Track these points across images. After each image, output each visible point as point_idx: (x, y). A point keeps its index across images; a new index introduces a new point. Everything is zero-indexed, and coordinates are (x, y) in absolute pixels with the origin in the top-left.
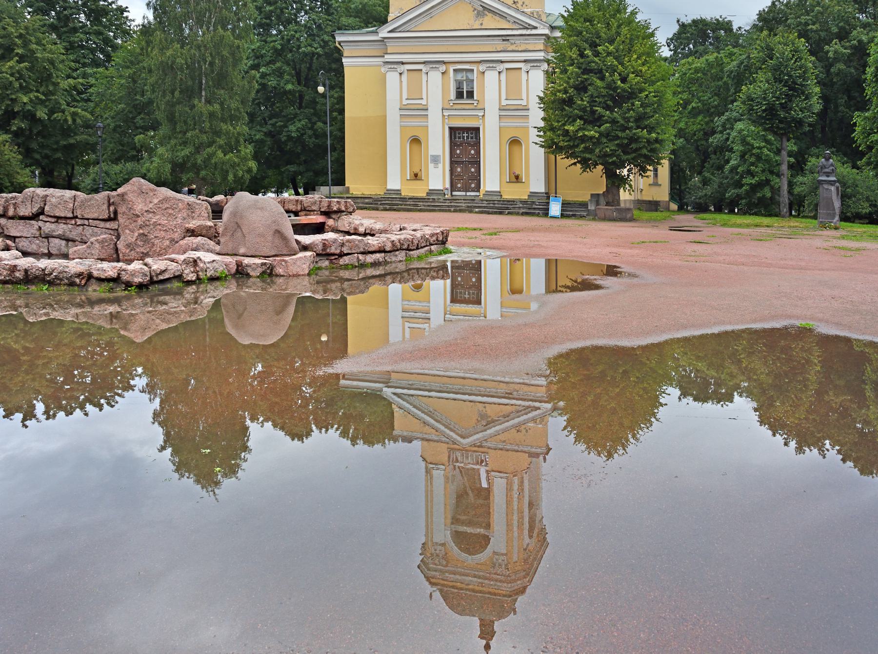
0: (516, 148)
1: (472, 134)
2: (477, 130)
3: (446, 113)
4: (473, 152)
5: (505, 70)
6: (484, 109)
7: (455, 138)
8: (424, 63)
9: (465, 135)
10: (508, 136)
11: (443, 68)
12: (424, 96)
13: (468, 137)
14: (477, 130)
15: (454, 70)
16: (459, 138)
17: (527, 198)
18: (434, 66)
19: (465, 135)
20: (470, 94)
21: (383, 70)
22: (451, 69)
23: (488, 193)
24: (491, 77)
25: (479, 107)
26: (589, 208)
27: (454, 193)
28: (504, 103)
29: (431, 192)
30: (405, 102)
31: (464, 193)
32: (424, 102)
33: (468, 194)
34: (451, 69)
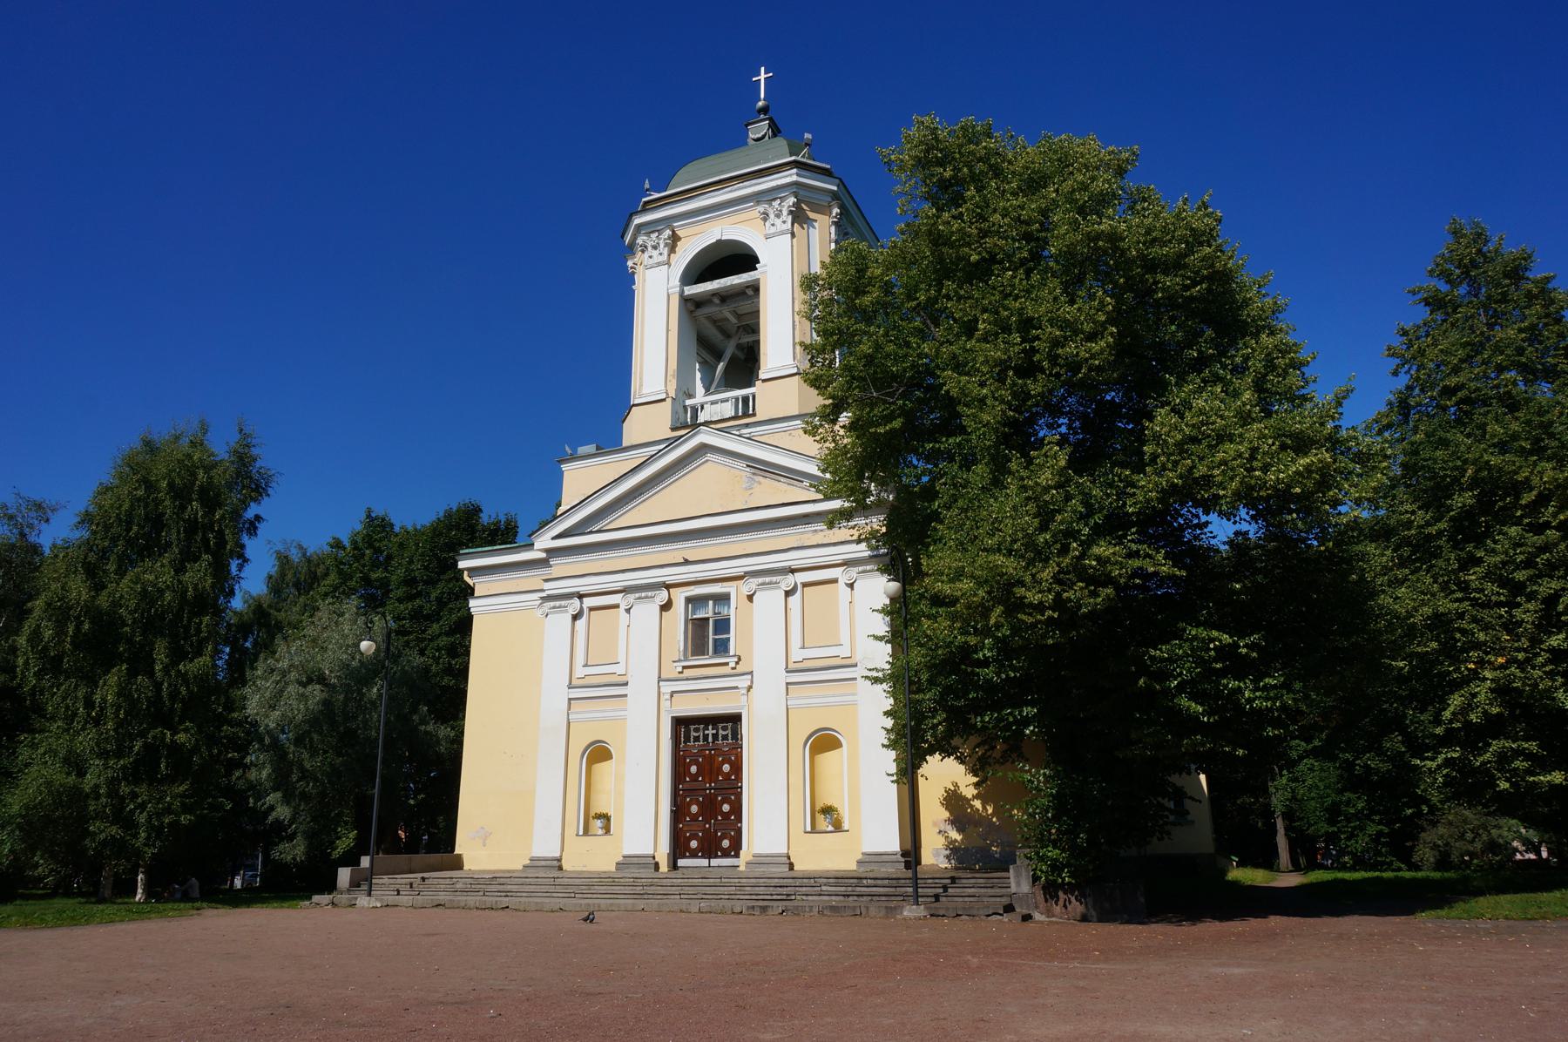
0: (828, 759)
1: (724, 729)
2: (735, 719)
3: (667, 688)
4: (726, 768)
5: (799, 586)
6: (751, 673)
7: (687, 739)
8: (625, 590)
9: (710, 732)
10: (804, 727)
11: (663, 595)
12: (621, 658)
13: (715, 736)
14: (735, 719)
15: (689, 600)
16: (697, 739)
17: (853, 867)
18: (643, 594)
19: (710, 732)
20: (722, 647)
21: (539, 612)
22: (679, 596)
23: (759, 861)
24: (770, 601)
25: (740, 669)
26: (1013, 889)
27: (681, 862)
28: (797, 654)
29: (627, 863)
30: (580, 671)
31: (704, 862)
32: (619, 669)
33: (714, 862)
34: (679, 596)
